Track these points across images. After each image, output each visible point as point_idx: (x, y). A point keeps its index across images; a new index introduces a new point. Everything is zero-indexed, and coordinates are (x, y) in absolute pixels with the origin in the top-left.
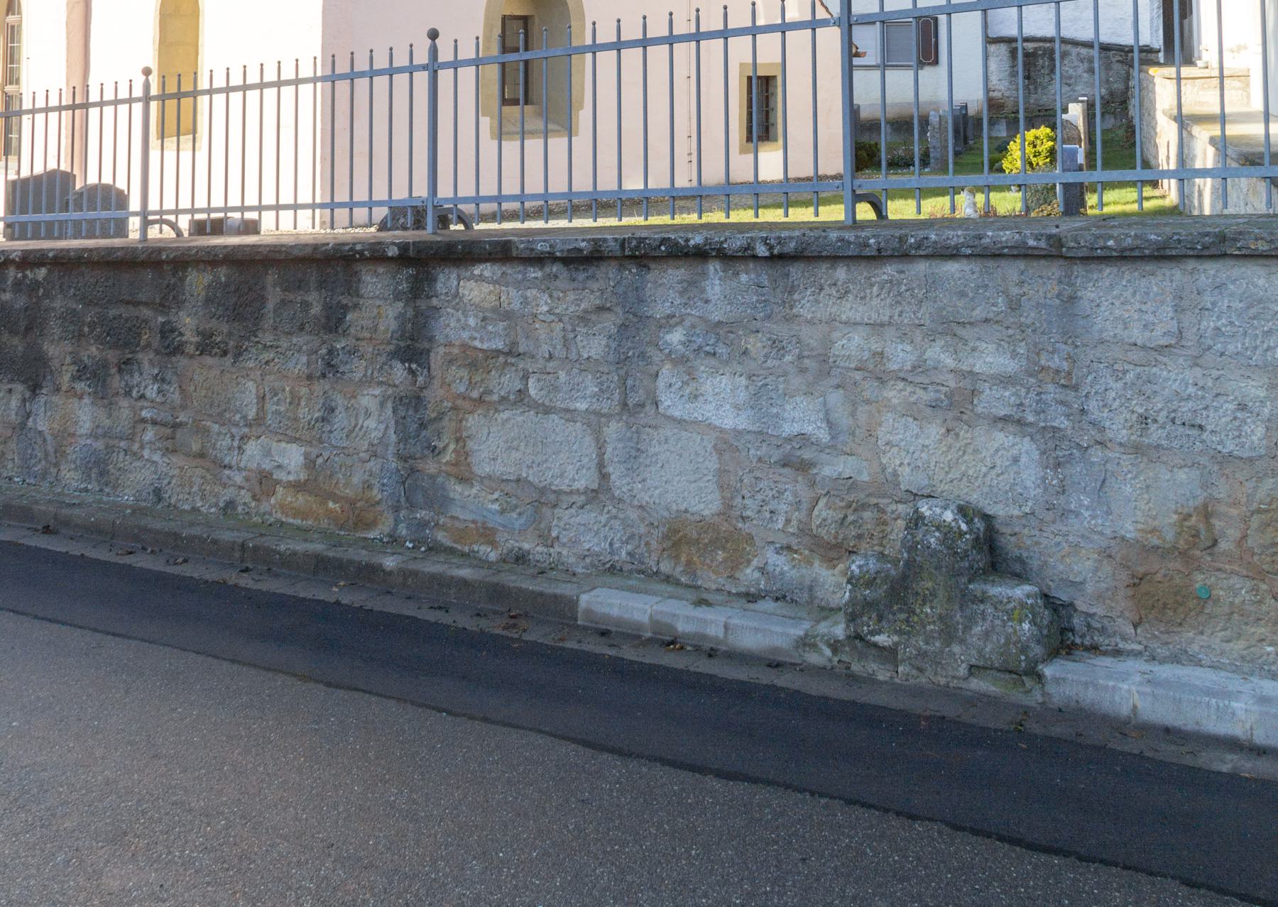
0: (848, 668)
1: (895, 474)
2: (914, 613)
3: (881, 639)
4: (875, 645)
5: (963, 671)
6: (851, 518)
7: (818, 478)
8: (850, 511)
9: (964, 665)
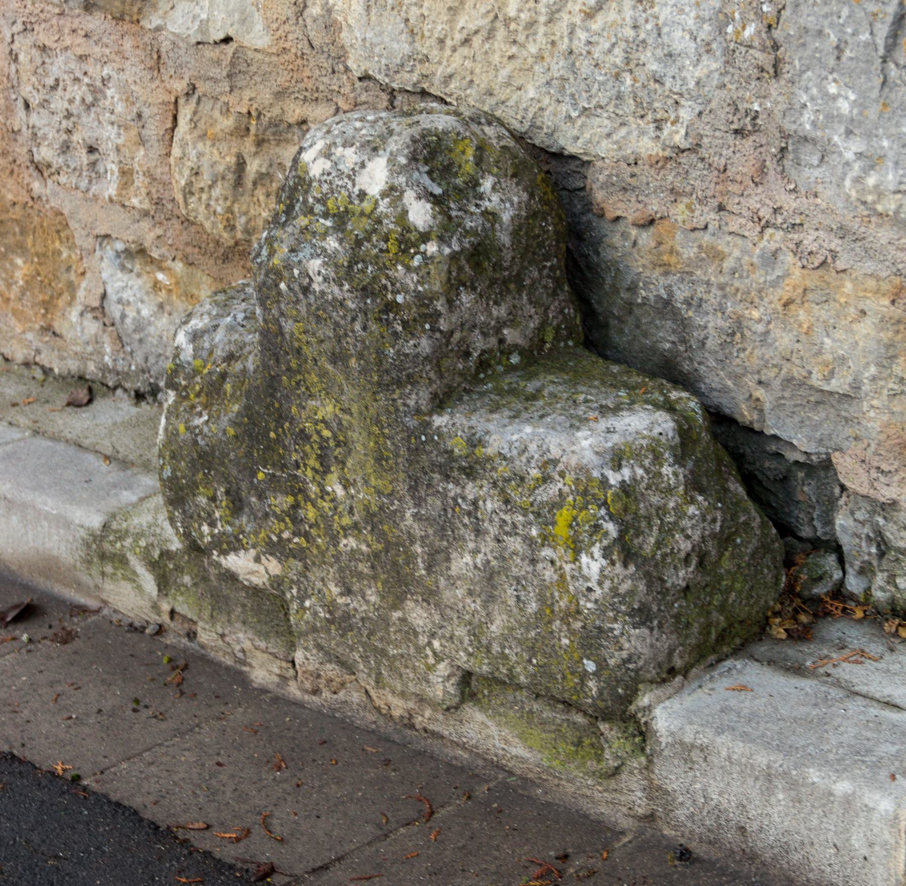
5: (441, 685)
9: (443, 668)
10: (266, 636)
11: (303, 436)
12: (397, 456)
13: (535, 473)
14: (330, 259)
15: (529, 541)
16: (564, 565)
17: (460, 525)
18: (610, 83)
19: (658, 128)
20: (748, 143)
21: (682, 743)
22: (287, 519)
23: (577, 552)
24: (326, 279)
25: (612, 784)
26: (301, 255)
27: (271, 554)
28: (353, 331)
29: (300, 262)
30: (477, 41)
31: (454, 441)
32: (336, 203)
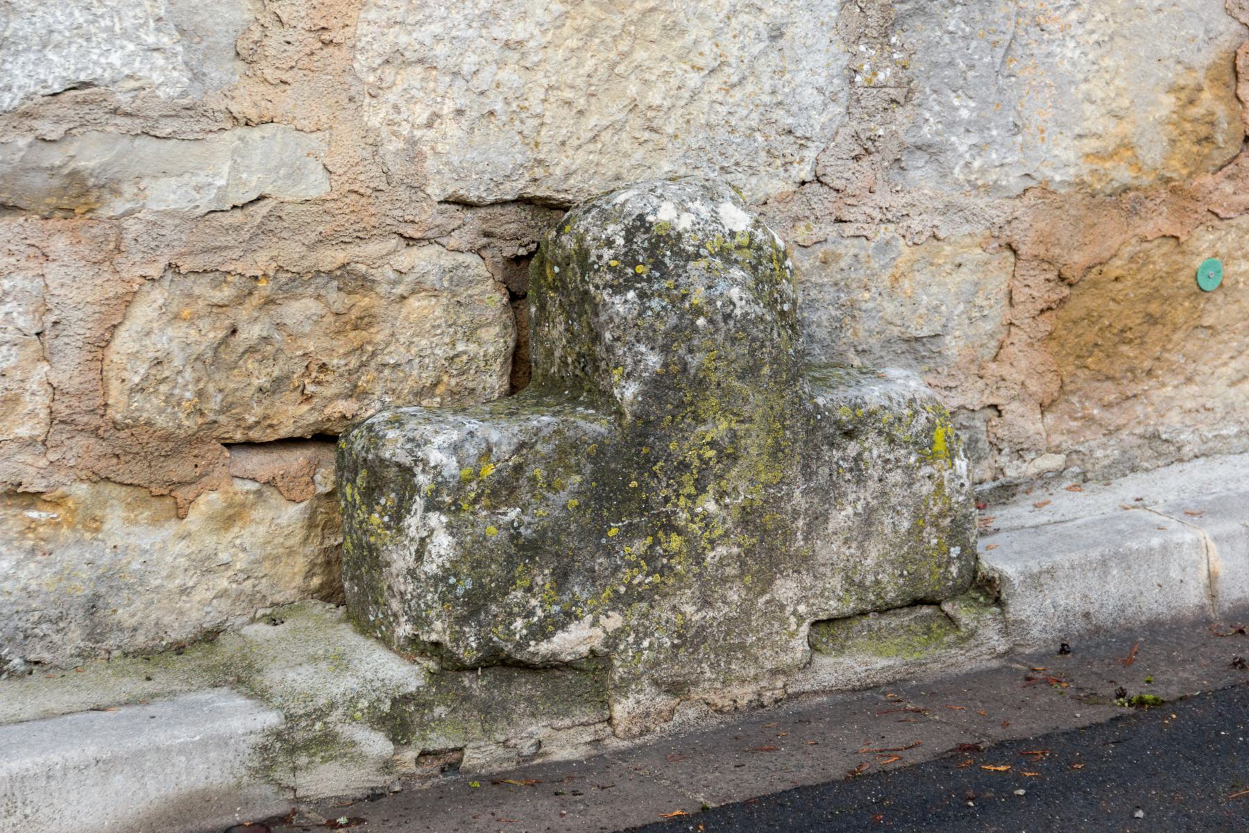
0: (454, 767)
1: (413, 153)
2: (670, 527)
3: (573, 640)
4: (552, 666)
6: (251, 333)
7: (133, 227)
8: (242, 314)
9: (805, 629)
10: (566, 714)
11: (684, 466)
12: (796, 441)
13: (907, 412)
14: (742, 284)
15: (908, 469)
16: (944, 473)
17: (843, 483)
18: (746, 143)
19: (786, 171)
20: (865, 162)
21: (1032, 576)
22: (643, 563)
23: (952, 458)
24: (748, 302)
25: (972, 642)
26: (720, 289)
27: (613, 610)
28: (772, 340)
29: (721, 294)
30: (606, 136)
31: (840, 412)
32: (713, 245)
